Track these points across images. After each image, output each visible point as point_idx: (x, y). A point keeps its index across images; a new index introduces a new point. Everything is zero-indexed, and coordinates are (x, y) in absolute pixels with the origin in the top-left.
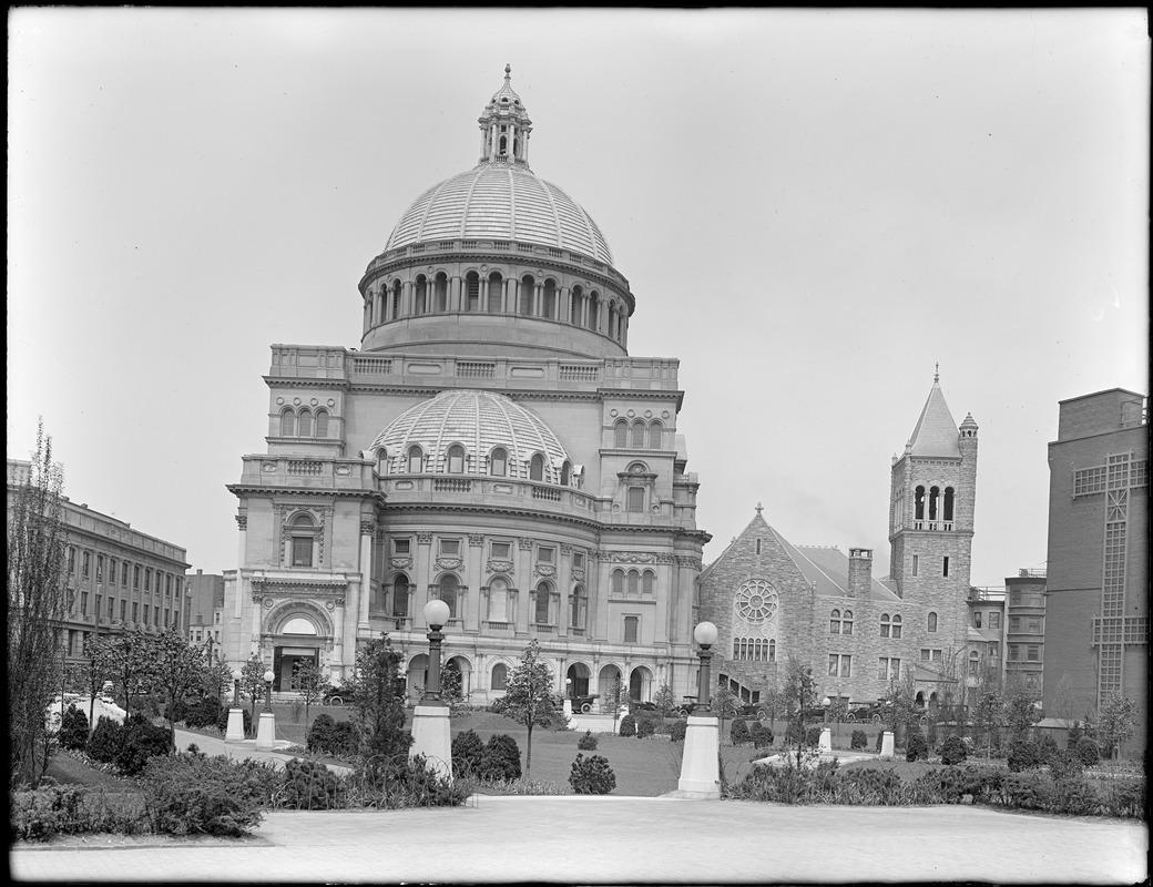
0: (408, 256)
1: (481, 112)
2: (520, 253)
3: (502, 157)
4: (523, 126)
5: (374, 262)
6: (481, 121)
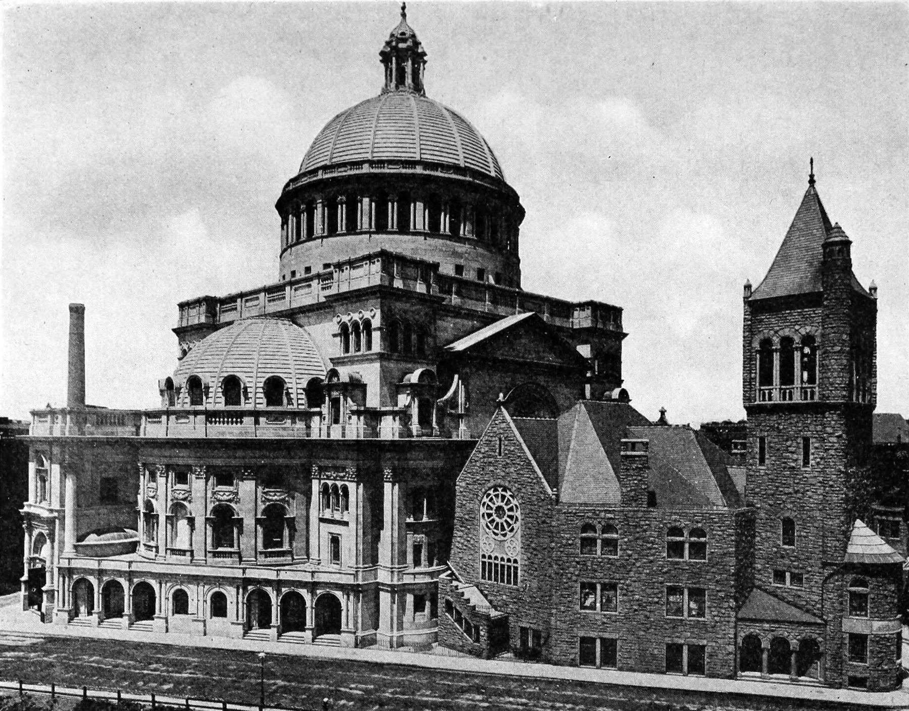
0: (320, 177)
1: (381, 46)
2: (427, 172)
3: (401, 81)
4: (419, 58)
5: (288, 185)
6: (382, 53)
